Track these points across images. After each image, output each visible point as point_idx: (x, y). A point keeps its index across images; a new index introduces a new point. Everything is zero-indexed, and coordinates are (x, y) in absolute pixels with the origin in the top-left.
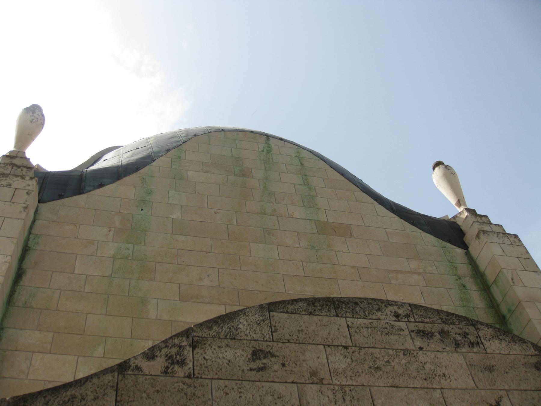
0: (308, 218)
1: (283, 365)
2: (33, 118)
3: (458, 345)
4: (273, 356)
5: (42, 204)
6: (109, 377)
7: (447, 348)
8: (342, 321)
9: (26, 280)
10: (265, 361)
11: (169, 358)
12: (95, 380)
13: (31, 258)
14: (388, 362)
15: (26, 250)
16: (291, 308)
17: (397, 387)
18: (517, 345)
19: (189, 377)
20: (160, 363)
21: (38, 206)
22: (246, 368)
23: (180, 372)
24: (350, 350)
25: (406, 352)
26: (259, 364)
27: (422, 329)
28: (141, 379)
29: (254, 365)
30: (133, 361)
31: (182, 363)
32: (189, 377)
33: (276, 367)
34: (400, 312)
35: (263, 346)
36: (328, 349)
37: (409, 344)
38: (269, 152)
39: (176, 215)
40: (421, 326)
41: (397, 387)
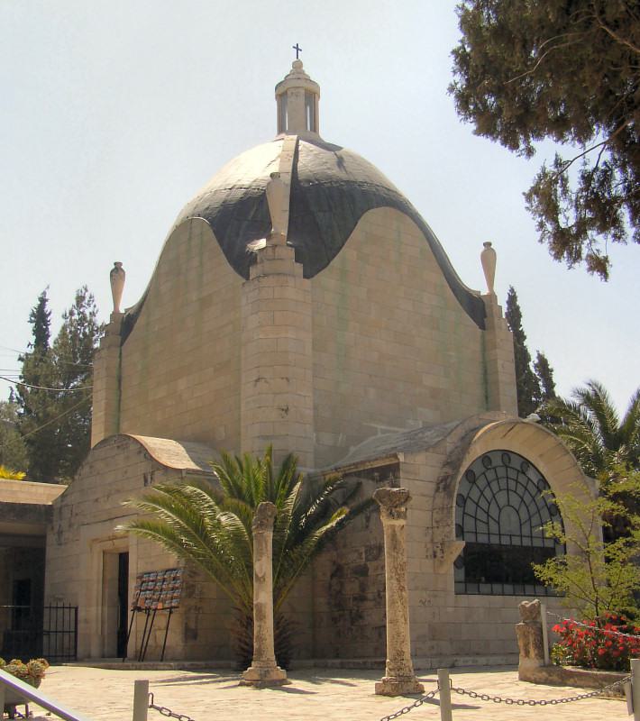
38: (190, 239)
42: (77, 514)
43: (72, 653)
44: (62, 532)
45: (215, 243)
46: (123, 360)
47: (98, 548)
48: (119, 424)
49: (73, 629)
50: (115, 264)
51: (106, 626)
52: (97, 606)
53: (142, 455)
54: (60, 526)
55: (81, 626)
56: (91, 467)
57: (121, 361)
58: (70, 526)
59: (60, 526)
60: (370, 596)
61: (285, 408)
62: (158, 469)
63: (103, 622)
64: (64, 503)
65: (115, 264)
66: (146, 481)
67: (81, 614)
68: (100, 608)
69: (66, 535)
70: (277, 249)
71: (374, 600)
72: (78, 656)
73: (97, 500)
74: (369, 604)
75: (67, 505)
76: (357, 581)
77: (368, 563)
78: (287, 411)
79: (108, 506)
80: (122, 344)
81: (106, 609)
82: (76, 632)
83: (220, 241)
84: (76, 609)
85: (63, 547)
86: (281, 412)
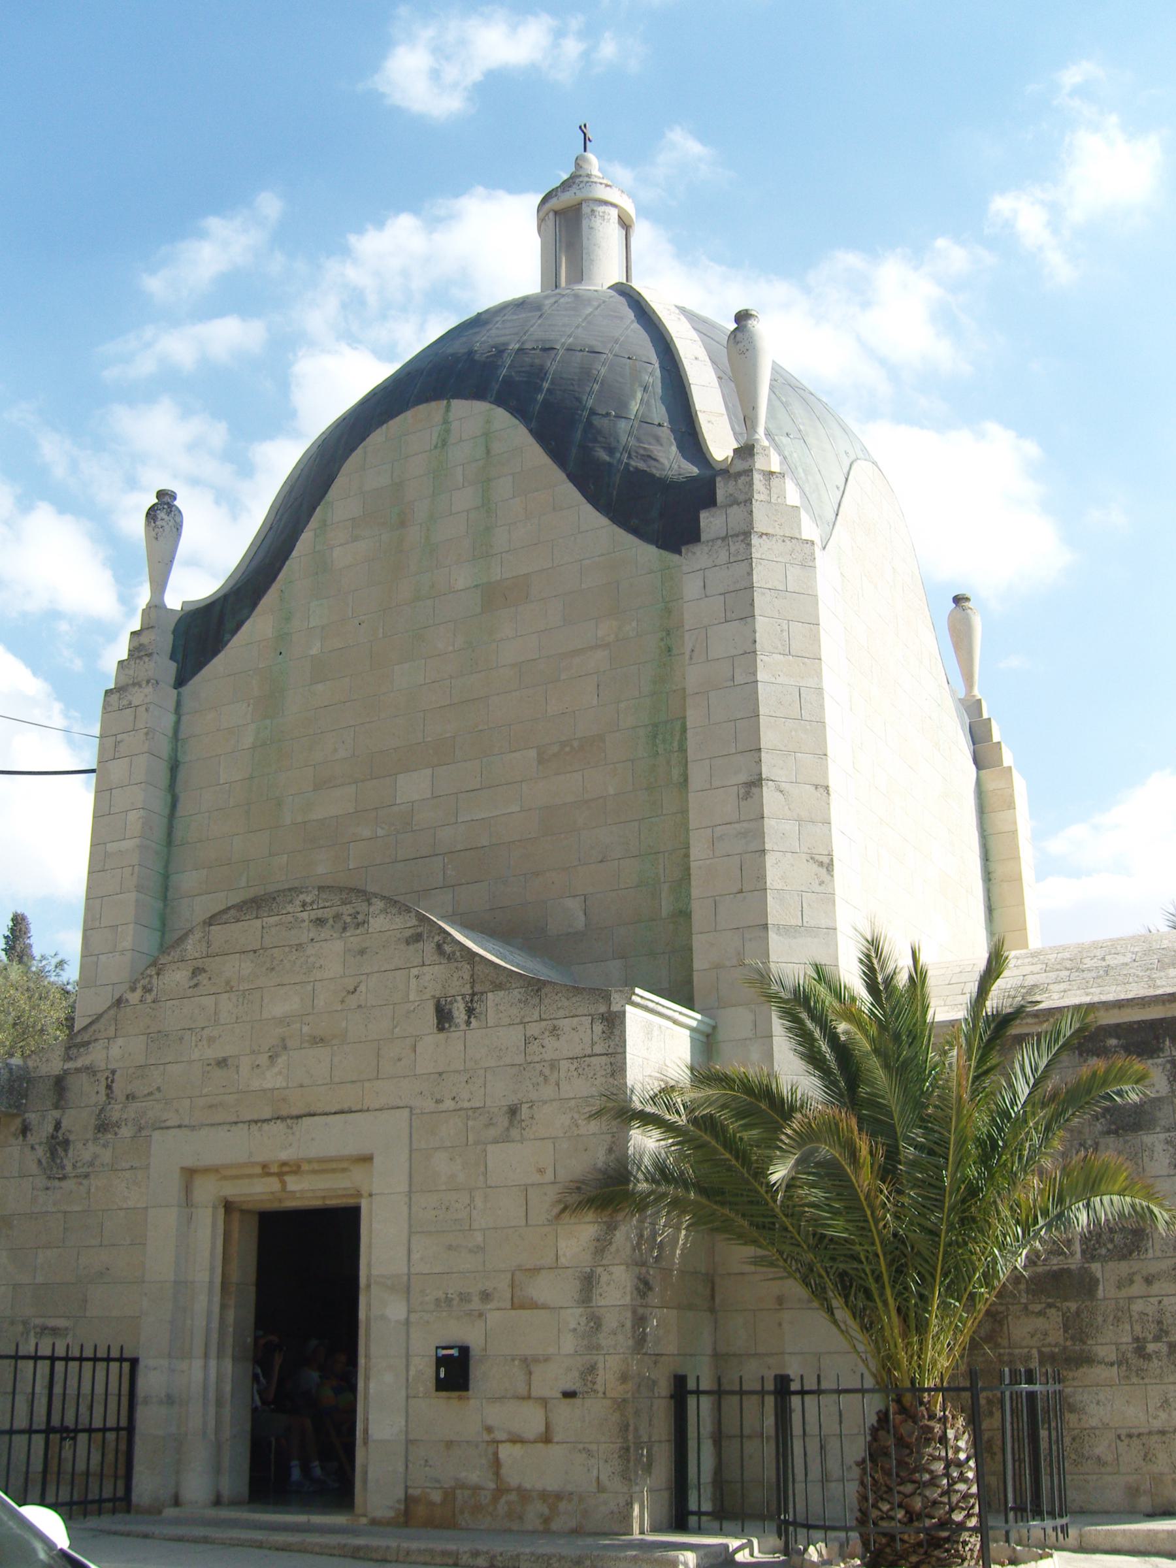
0: (475, 583)
1: (210, 979)
2: (157, 530)
3: (344, 929)
4: (204, 970)
5: (184, 688)
6: (112, 1012)
7: (335, 935)
8: (258, 923)
9: (180, 812)
10: (199, 978)
11: (144, 987)
12: (105, 1016)
13: (182, 775)
14: (282, 960)
15: (174, 767)
16: (225, 917)
17: (283, 985)
18: (401, 917)
19: (154, 1002)
20: (139, 993)
21: (179, 694)
22: (187, 986)
23: (149, 998)
24: (257, 954)
25: (299, 947)
26: (195, 981)
27: (320, 916)
28: (128, 1009)
29: (192, 983)
30: (125, 995)
31: (150, 991)
32: (154, 1002)
33: (205, 982)
34: (308, 899)
35: (199, 964)
36: (243, 956)
37: (304, 938)
38: (444, 443)
39: (314, 651)
40: (320, 913)
41: (283, 985)
42: (130, 1097)
43: (120, 1493)
44: (66, 1143)
45: (535, 455)
46: (184, 719)
47: (208, 1191)
48: (166, 877)
49: (124, 1423)
50: (161, 494)
51: (227, 1411)
52: (206, 1356)
53: (429, 947)
54: (58, 1126)
55: (149, 1420)
56: (197, 972)
57: (178, 723)
58: (103, 1127)
59: (58, 1126)
60: (1105, 1351)
61: (826, 860)
62: (498, 987)
63: (219, 1403)
64: (79, 1064)
65: (161, 494)
66: (443, 1017)
67: (151, 1381)
68: (213, 1363)
69: (83, 1152)
70: (775, 482)
71: (1121, 1362)
72: (135, 1498)
73: (222, 1063)
74: (1100, 1373)
75: (90, 1070)
76: (1053, 1311)
77: (1096, 1267)
78: (829, 867)
79: (272, 1079)
80: (180, 681)
81: (228, 1365)
82: (130, 1429)
83: (558, 455)
84: (134, 1362)
85: (69, 1184)
86: (815, 868)
